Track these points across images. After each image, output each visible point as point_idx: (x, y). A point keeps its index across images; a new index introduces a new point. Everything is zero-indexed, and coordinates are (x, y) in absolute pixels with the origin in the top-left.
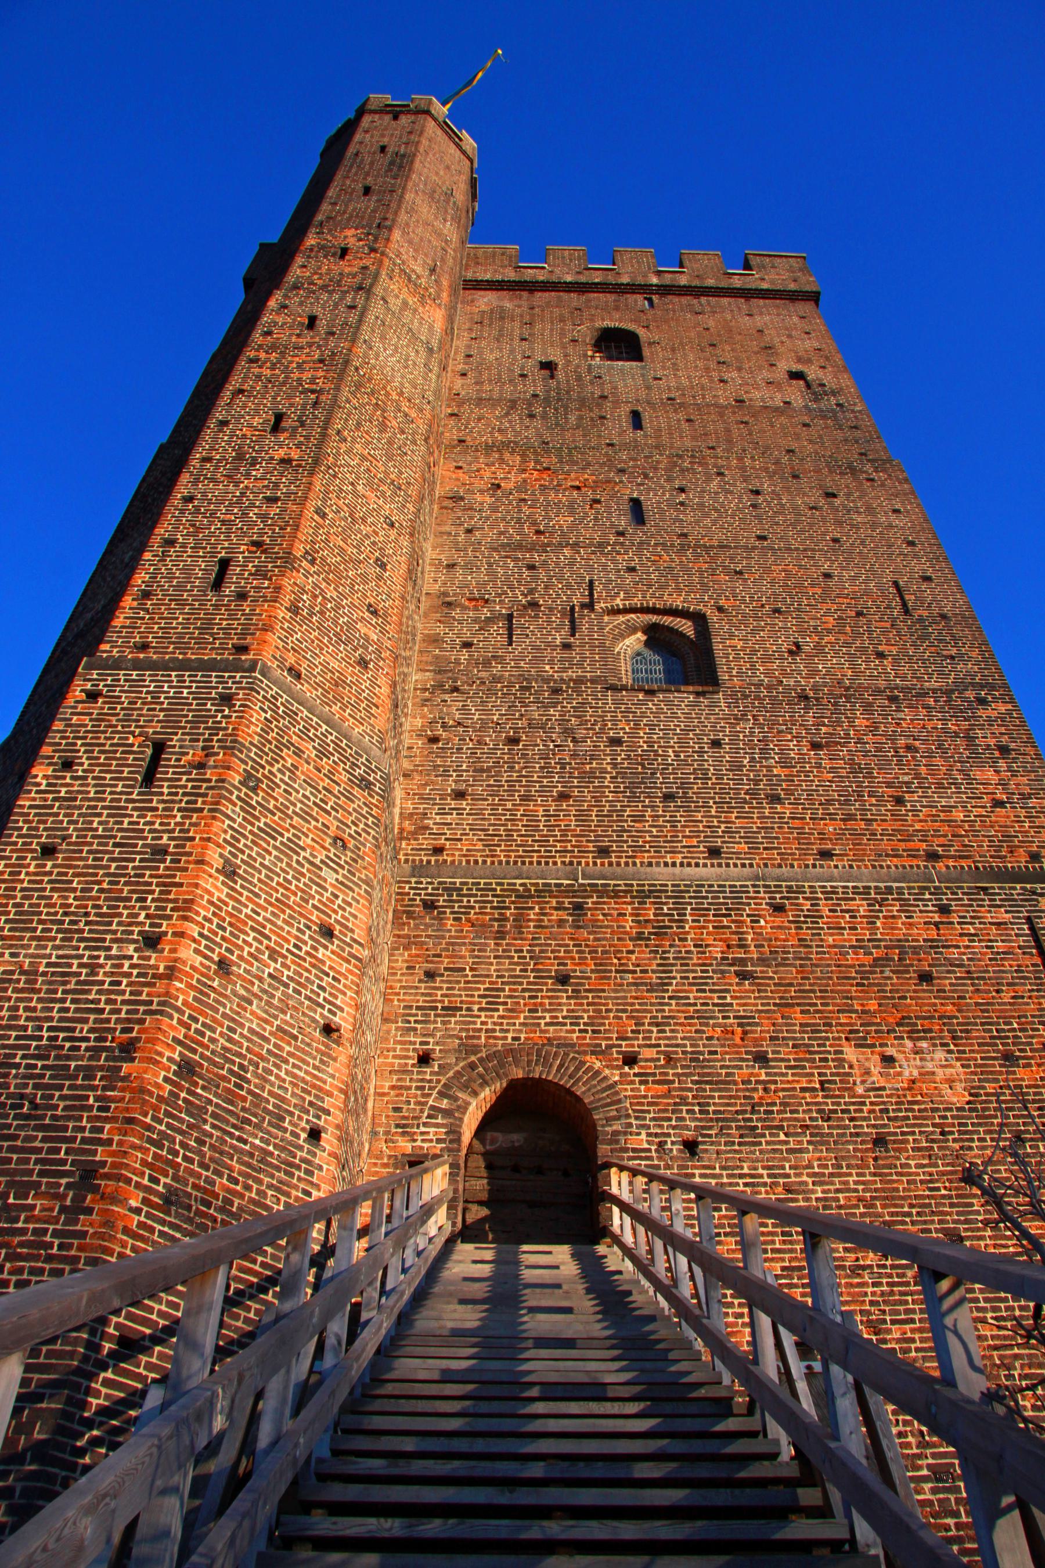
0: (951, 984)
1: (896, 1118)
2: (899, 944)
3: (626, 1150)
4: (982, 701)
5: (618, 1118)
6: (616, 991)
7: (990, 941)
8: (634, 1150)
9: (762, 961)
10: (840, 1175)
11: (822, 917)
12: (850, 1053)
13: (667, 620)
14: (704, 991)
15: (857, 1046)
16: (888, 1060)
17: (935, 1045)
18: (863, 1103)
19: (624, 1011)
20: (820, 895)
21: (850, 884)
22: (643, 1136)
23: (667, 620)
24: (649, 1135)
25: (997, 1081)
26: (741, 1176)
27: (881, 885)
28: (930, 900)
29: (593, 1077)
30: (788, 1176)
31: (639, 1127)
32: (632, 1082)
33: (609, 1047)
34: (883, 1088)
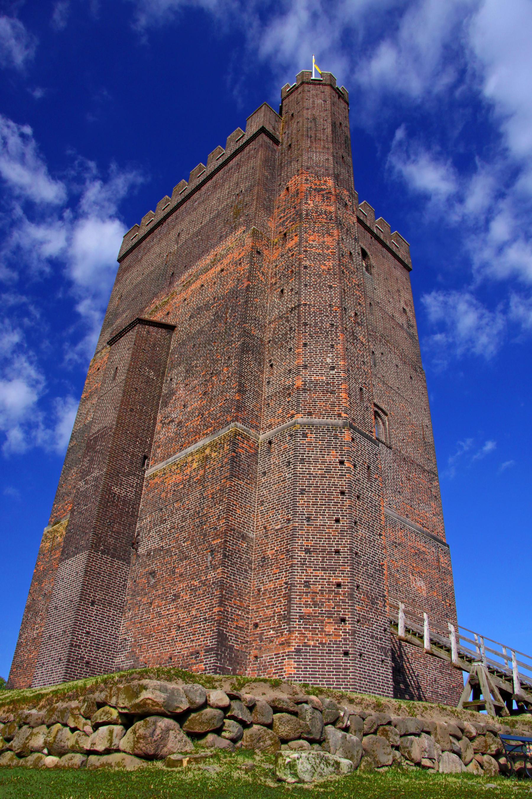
12: (411, 576)
13: (380, 412)
23: (380, 412)
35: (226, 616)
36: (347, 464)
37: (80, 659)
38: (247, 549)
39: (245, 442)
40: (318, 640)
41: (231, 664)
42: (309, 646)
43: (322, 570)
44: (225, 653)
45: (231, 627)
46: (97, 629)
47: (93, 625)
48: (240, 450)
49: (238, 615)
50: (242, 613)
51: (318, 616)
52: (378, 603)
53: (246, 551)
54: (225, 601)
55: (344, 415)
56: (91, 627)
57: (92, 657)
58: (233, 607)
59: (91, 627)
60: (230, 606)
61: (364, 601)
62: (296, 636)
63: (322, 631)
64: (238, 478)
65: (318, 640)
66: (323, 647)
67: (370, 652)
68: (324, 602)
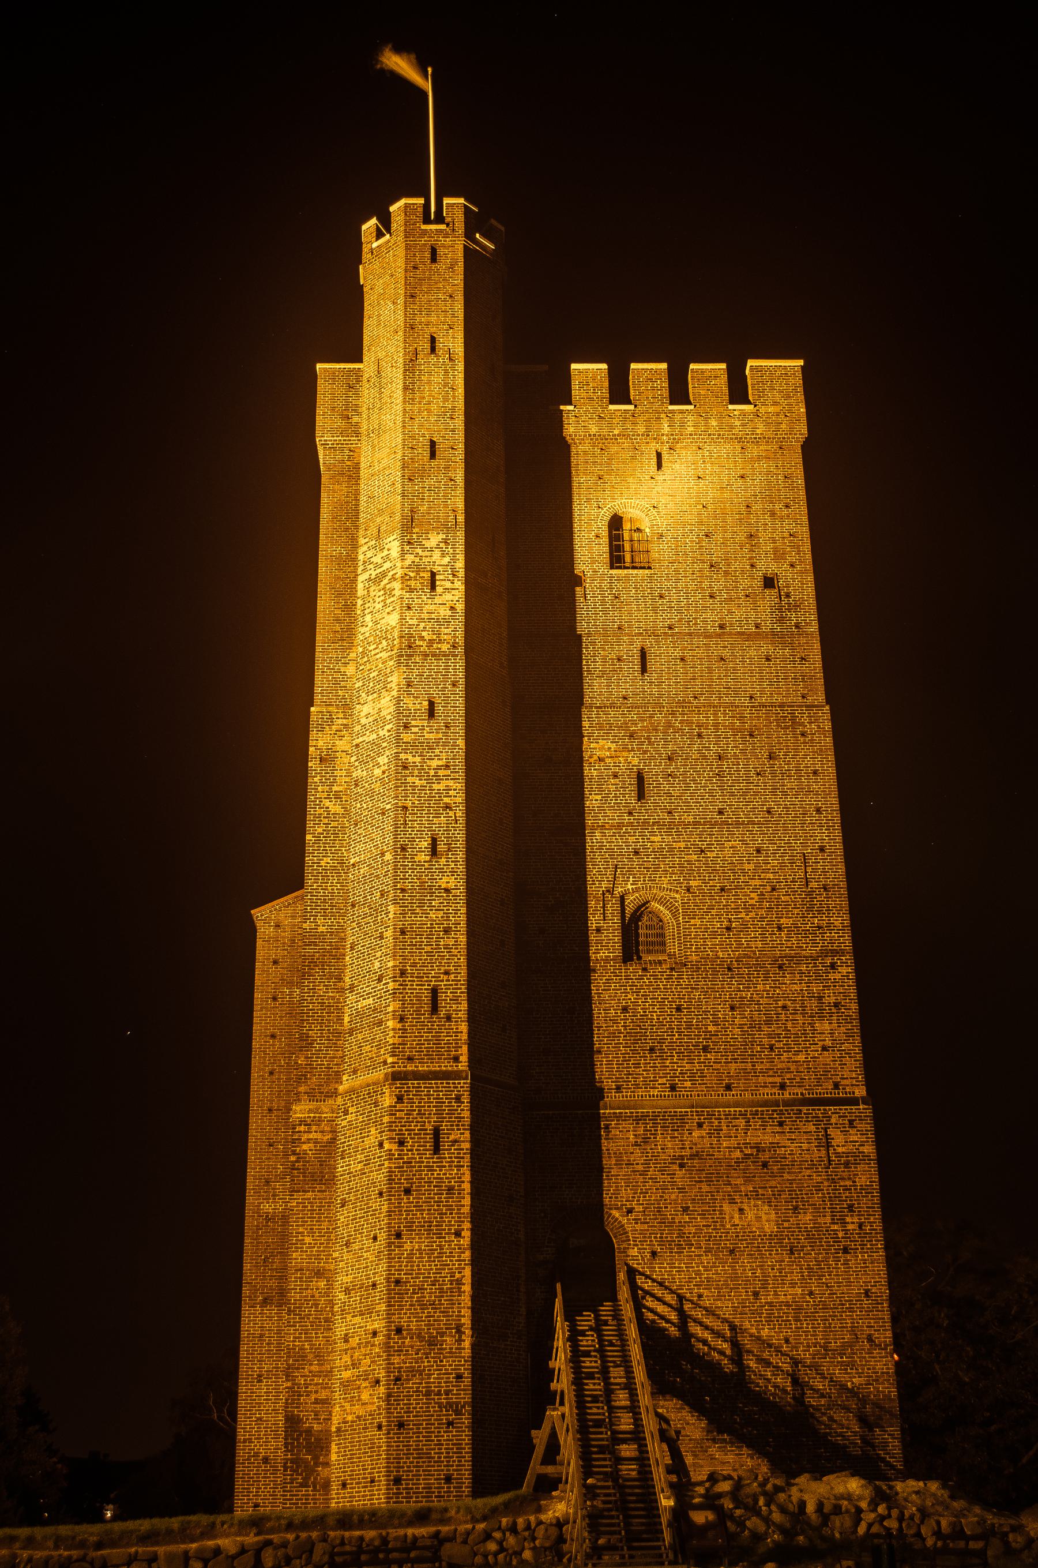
0: (778, 1169)
1: (742, 1240)
2: (758, 1148)
3: (629, 1256)
4: (833, 966)
5: (624, 1241)
6: (625, 1175)
7: (801, 1143)
8: (632, 1256)
9: (692, 1157)
10: (715, 1267)
11: (722, 1130)
12: (726, 1207)
14: (664, 1174)
15: (730, 1203)
16: (741, 1210)
17: (764, 1202)
18: (729, 1233)
19: (628, 1186)
20: (722, 1117)
21: (738, 1109)
22: (636, 1249)
24: (638, 1249)
25: (789, 1221)
26: (675, 1267)
27: (754, 1109)
28: (776, 1118)
29: (615, 1221)
30: (693, 1267)
31: (634, 1245)
32: (631, 1223)
33: (622, 1205)
34: (738, 1225)
35: (297, 1392)
36: (386, 1146)
37: (253, 1456)
38: (327, 1289)
39: (314, 1128)
40: (355, 1413)
41: (308, 1453)
42: (347, 1422)
43: (360, 1315)
44: (298, 1439)
45: (306, 1403)
46: (272, 1410)
47: (265, 1407)
48: (305, 1147)
49: (317, 1384)
50: (323, 1380)
51: (355, 1381)
52: (446, 1341)
53: (325, 1293)
54: (294, 1372)
55: (390, 1060)
56: (263, 1410)
57: (270, 1449)
58: (309, 1376)
59: (263, 1410)
60: (301, 1376)
61: (412, 1347)
62: (337, 1411)
63: (359, 1400)
64: (303, 1191)
65: (355, 1413)
66: (360, 1421)
67: (422, 1416)
68: (361, 1360)
